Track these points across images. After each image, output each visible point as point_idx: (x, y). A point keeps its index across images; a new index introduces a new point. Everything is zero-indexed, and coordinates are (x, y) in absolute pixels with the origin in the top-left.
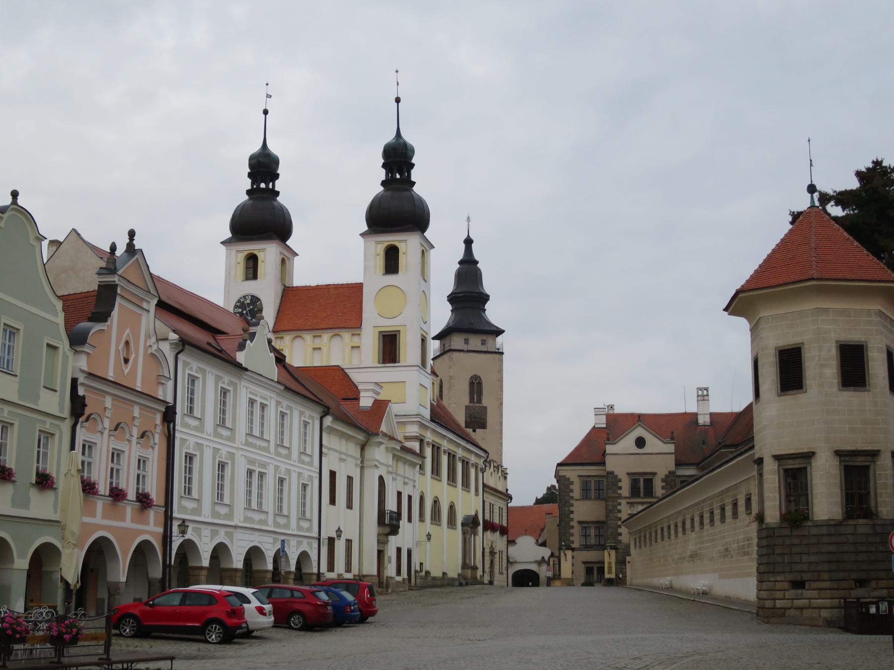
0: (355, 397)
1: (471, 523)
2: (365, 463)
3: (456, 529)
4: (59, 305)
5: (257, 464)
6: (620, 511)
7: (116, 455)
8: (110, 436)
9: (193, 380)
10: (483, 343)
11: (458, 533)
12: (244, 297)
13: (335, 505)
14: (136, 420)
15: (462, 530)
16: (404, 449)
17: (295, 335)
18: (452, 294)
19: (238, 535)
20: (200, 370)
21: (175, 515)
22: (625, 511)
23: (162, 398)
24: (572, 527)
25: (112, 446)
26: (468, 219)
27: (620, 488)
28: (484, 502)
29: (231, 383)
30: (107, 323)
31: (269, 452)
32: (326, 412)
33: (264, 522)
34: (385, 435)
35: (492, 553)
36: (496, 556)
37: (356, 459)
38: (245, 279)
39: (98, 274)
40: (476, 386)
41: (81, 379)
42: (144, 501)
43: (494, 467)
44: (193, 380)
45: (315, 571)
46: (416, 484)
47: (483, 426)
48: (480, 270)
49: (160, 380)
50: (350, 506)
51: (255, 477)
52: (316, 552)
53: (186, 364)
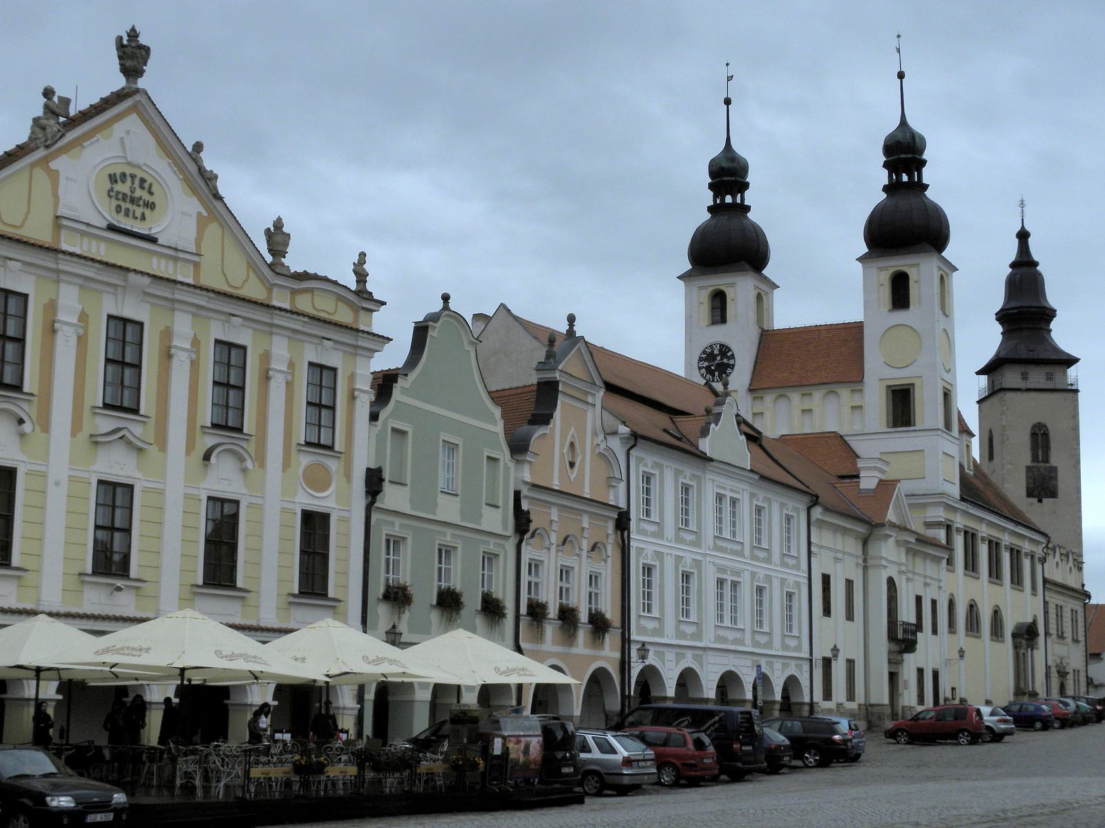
0: (855, 474)
1: (1027, 635)
2: (869, 561)
3: (1003, 642)
4: (497, 412)
5: (729, 572)
7: (565, 573)
8: (558, 551)
9: (648, 478)
10: (1049, 377)
11: (1006, 648)
12: (711, 346)
13: (830, 616)
14: (586, 531)
15: (1014, 643)
16: (922, 540)
18: (1002, 310)
19: (711, 658)
20: (656, 465)
21: (632, 637)
23: (612, 503)
25: (560, 563)
26: (1022, 204)
28: (1046, 603)
29: (694, 477)
30: (549, 426)
31: (743, 556)
32: (815, 500)
33: (740, 642)
34: (893, 525)
35: (1062, 674)
36: (1068, 677)
37: (857, 557)
38: (711, 322)
39: (537, 370)
40: (1040, 438)
41: (525, 491)
42: (599, 624)
43: (1061, 554)
44: (648, 478)
45: (807, 699)
47: (1053, 494)
48: (1040, 274)
49: (610, 482)
50: (850, 616)
51: (727, 587)
52: (807, 675)
53: (639, 460)
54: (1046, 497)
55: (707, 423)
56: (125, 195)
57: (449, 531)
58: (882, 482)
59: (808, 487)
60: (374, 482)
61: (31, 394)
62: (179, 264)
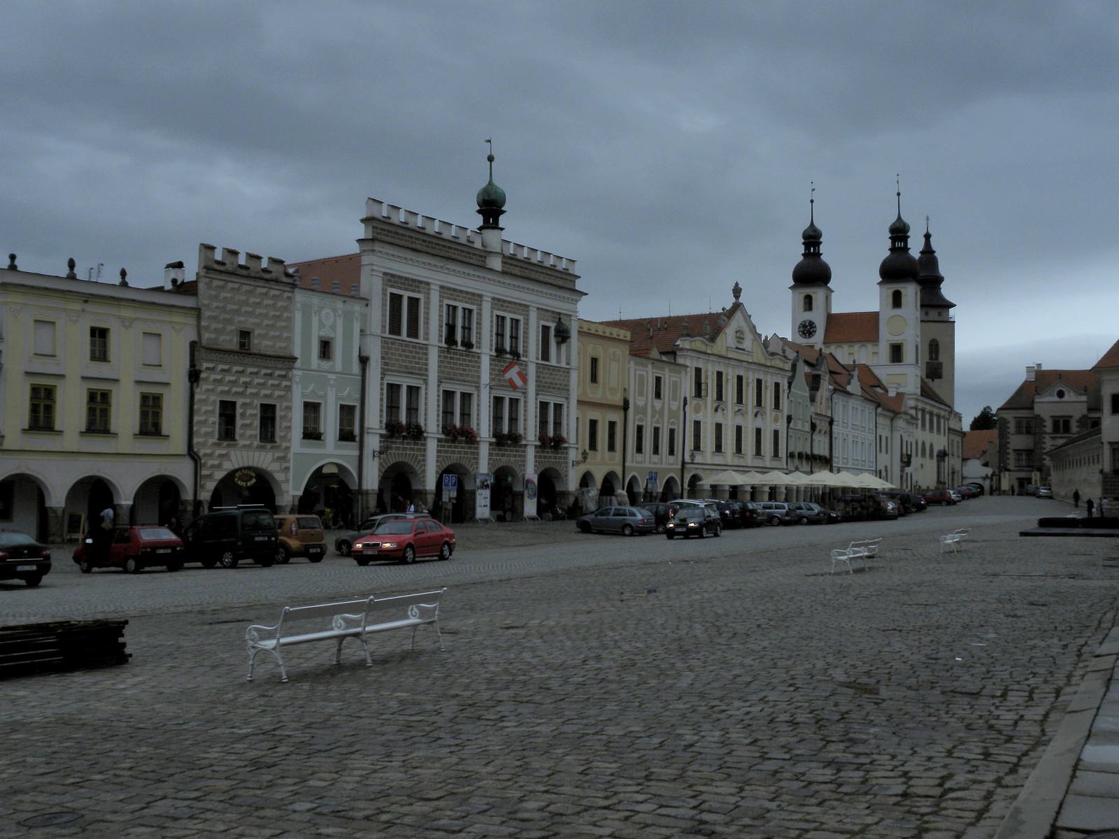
1: (942, 455)
6: (1044, 443)
10: (940, 314)
16: (912, 417)
22: (1048, 444)
24: (1009, 454)
26: (928, 219)
27: (1045, 426)
32: (879, 405)
33: (858, 465)
40: (934, 347)
41: (813, 416)
47: (940, 377)
50: (887, 453)
54: (937, 378)
58: (898, 394)
60: (789, 419)
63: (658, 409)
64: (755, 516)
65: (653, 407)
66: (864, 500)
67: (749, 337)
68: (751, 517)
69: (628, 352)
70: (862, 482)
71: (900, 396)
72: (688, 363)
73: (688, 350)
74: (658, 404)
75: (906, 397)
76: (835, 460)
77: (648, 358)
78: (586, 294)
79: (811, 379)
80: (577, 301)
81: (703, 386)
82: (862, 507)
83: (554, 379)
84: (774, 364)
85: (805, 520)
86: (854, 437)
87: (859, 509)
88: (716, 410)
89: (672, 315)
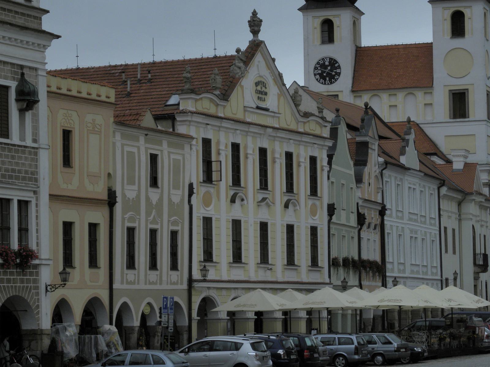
2: (462, 216)
12: (323, 59)
14: (374, 219)
17: (373, 94)
32: (442, 183)
33: (418, 272)
41: (360, 203)
46: (488, 224)
50: (454, 253)
55: (403, 147)
56: (260, 91)
57: (344, 228)
58: (466, 165)
59: (438, 175)
60: (331, 210)
61: (243, 187)
62: (275, 118)
63: (154, 203)
64: (316, 355)
65: (148, 198)
66: (451, 326)
67: (273, 90)
68: (311, 358)
69: (112, 120)
70: (450, 300)
71: (470, 167)
72: (193, 133)
73: (192, 113)
74: (154, 194)
75: (479, 168)
76: (388, 266)
77: (139, 127)
78: (58, 37)
79: (354, 147)
80: (45, 47)
81: (214, 166)
82: (453, 337)
83: (17, 164)
84: (308, 130)
85: (380, 358)
86: (411, 231)
87: (448, 340)
88: (233, 201)
89: (158, 59)
